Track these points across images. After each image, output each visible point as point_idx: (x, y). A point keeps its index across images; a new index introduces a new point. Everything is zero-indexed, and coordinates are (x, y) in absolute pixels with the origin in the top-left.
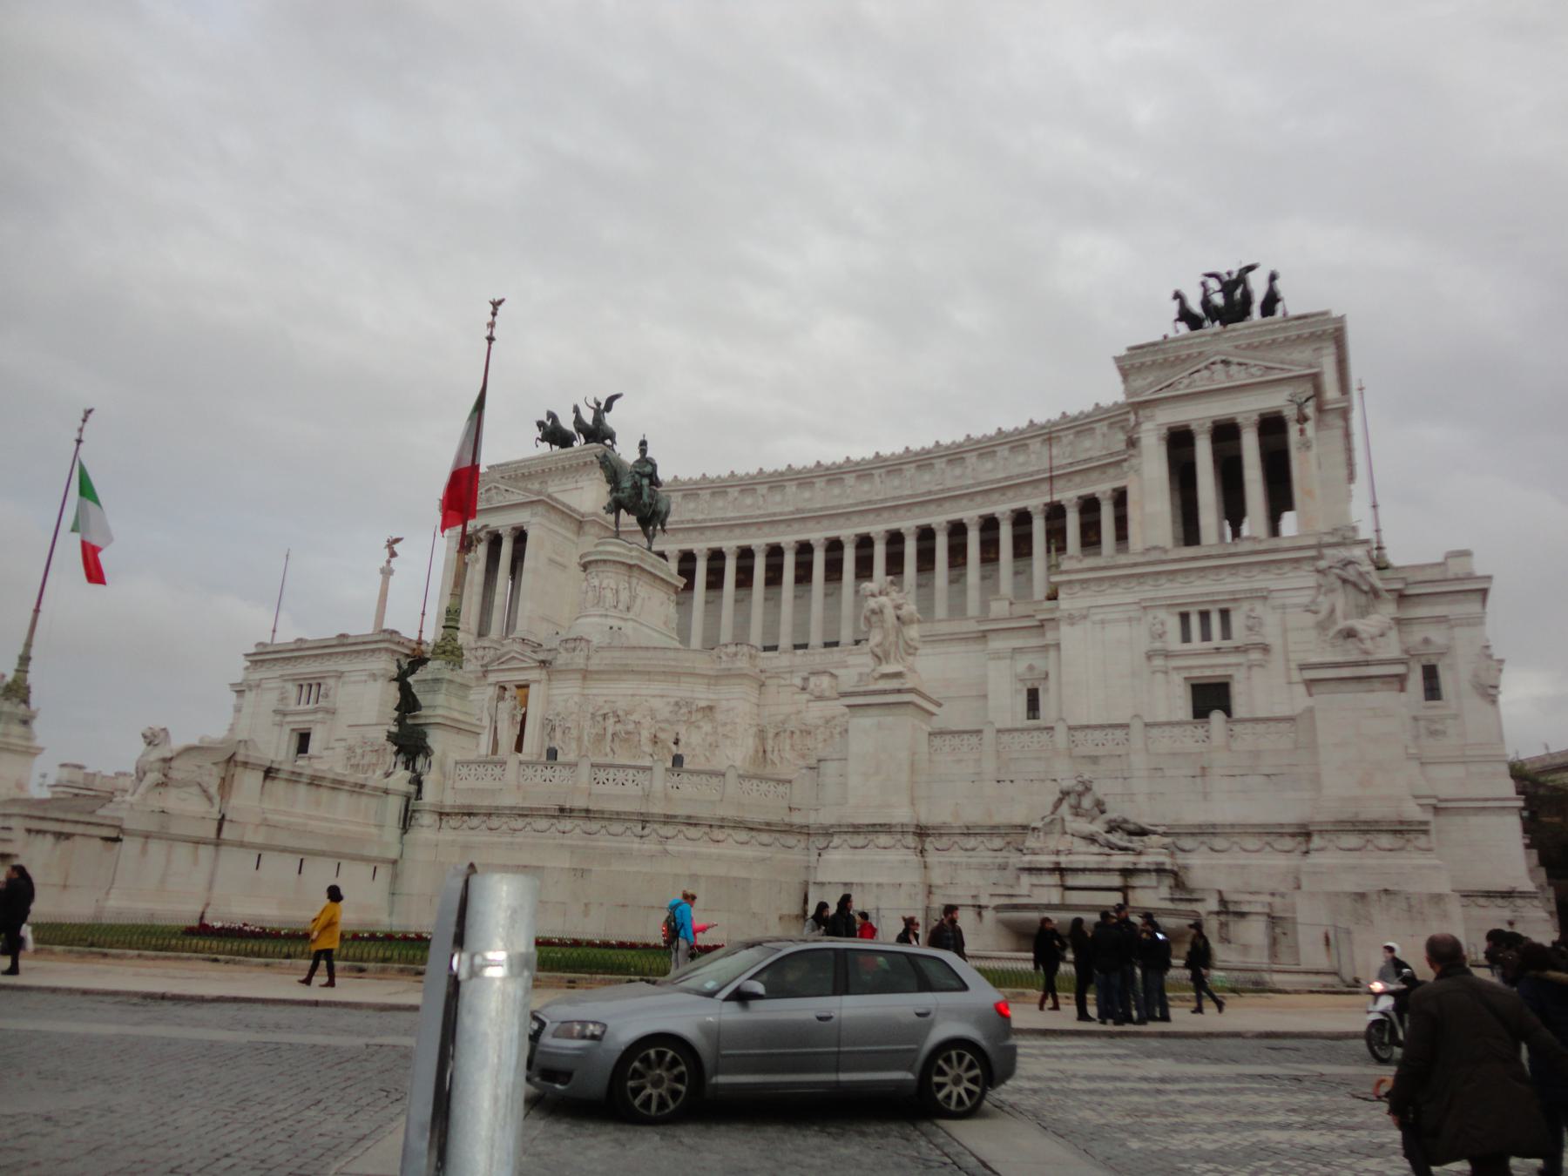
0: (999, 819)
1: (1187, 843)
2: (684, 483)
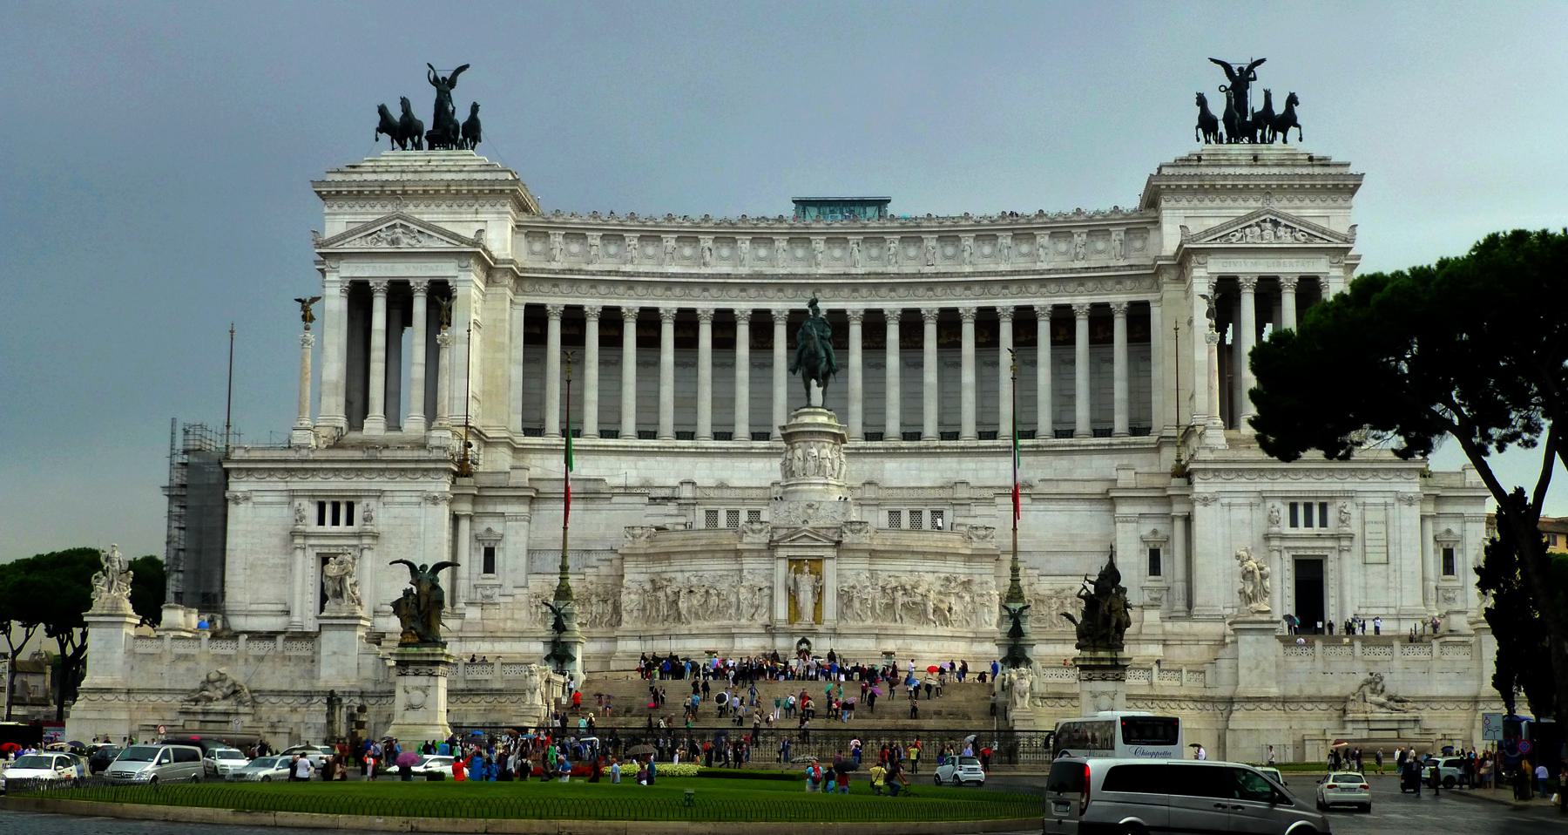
0: (1324, 693)
1: (1421, 706)
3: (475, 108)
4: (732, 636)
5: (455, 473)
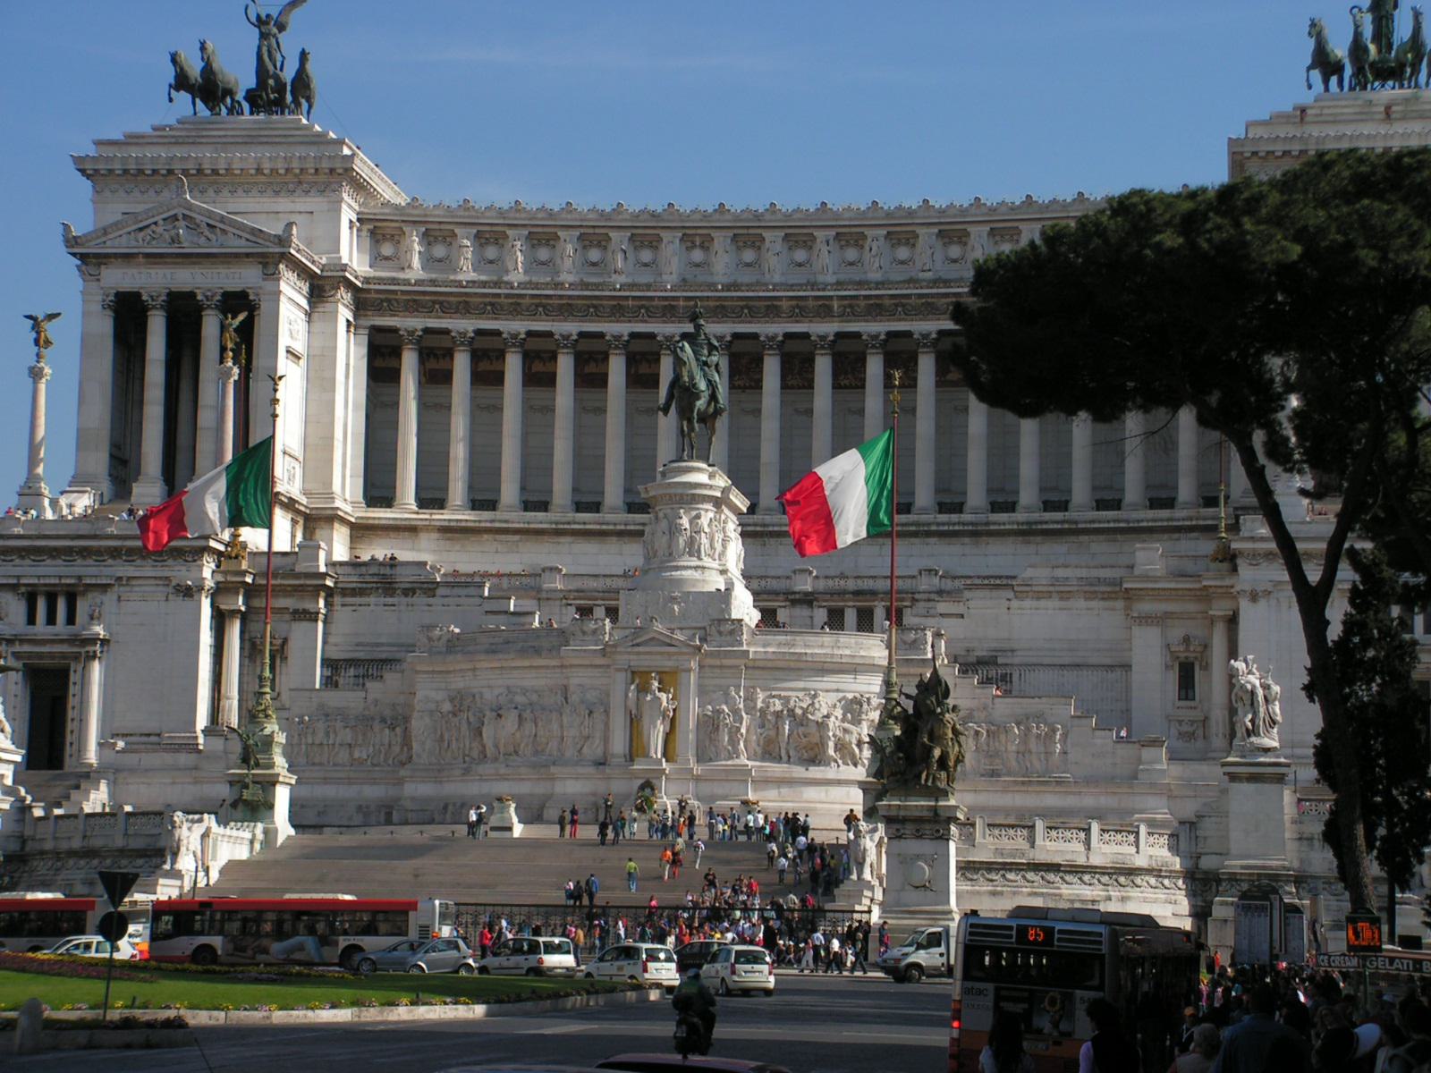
3: (303, 56)
5: (220, 554)
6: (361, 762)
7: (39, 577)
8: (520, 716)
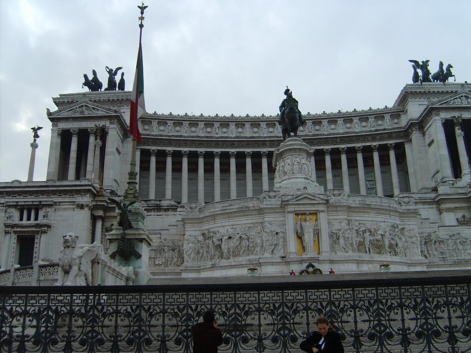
2: (175, 116)
3: (123, 74)
4: (260, 264)
5: (94, 196)
6: (159, 265)
7: (25, 202)
8: (240, 237)
